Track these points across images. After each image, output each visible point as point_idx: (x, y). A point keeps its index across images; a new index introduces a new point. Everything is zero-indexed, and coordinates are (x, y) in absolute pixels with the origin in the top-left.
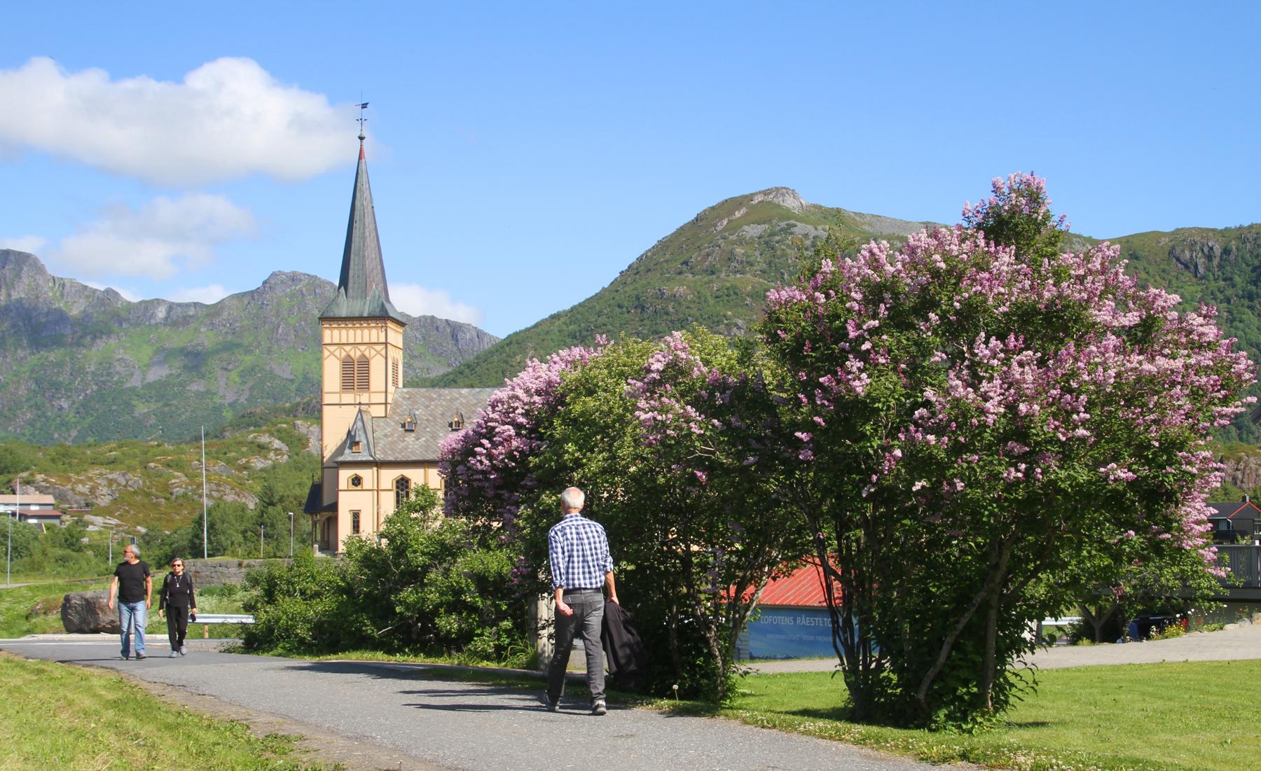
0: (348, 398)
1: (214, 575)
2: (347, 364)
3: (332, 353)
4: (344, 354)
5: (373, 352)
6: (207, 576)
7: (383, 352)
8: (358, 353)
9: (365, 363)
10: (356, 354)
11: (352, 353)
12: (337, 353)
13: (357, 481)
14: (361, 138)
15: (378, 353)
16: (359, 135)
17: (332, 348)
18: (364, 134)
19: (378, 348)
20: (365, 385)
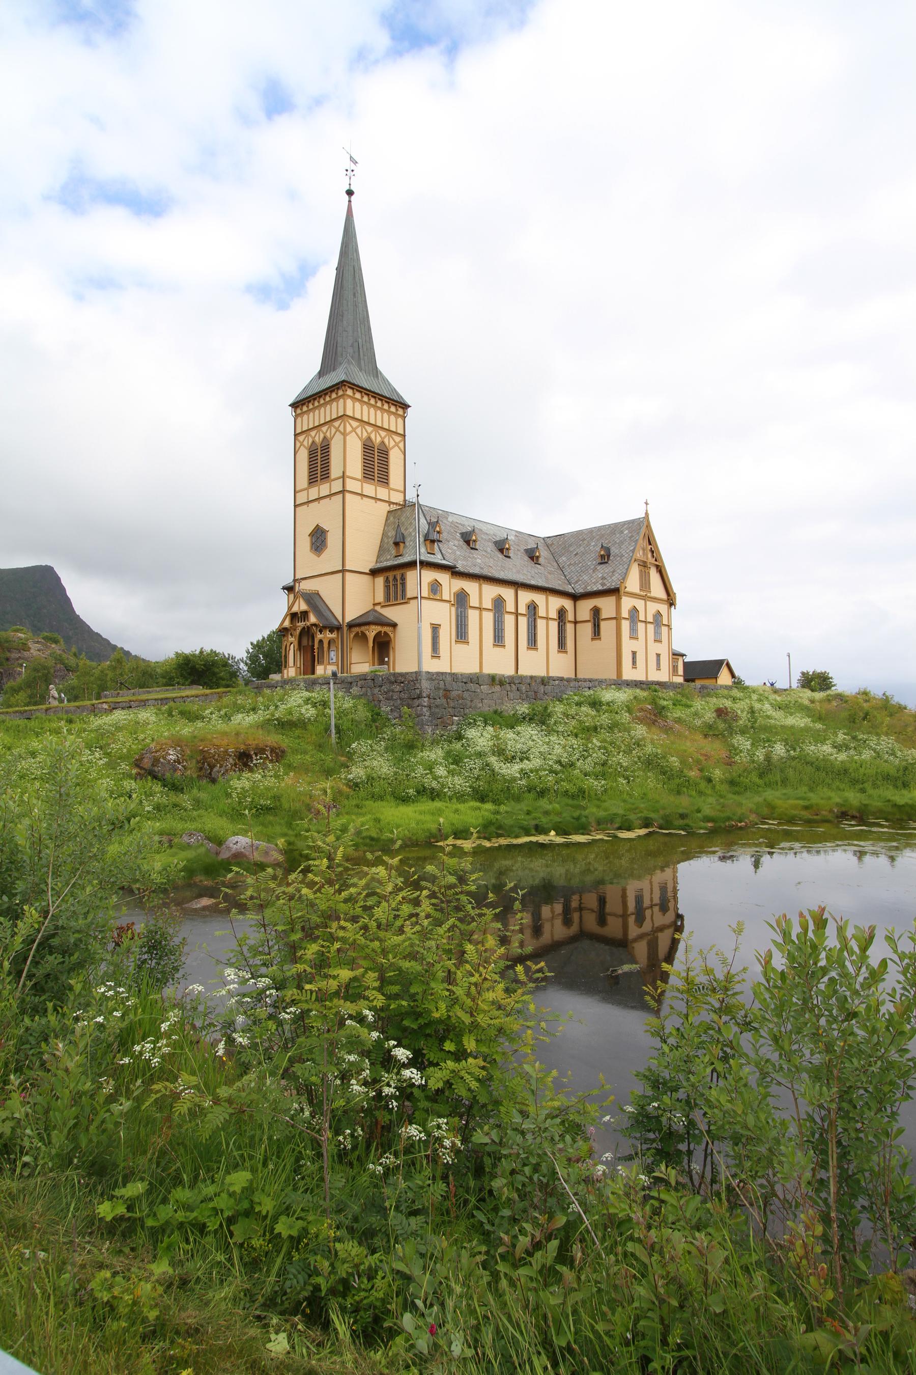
0: (369, 489)
1: (466, 695)
2: (367, 447)
3: (354, 430)
4: (365, 435)
5: (392, 443)
6: (458, 696)
7: (401, 445)
8: (379, 439)
9: (384, 453)
10: (377, 438)
11: (373, 436)
12: (359, 431)
13: (435, 587)
14: (350, 193)
15: (397, 444)
16: (347, 188)
17: (355, 424)
18: (353, 188)
19: (398, 439)
20: (384, 480)
